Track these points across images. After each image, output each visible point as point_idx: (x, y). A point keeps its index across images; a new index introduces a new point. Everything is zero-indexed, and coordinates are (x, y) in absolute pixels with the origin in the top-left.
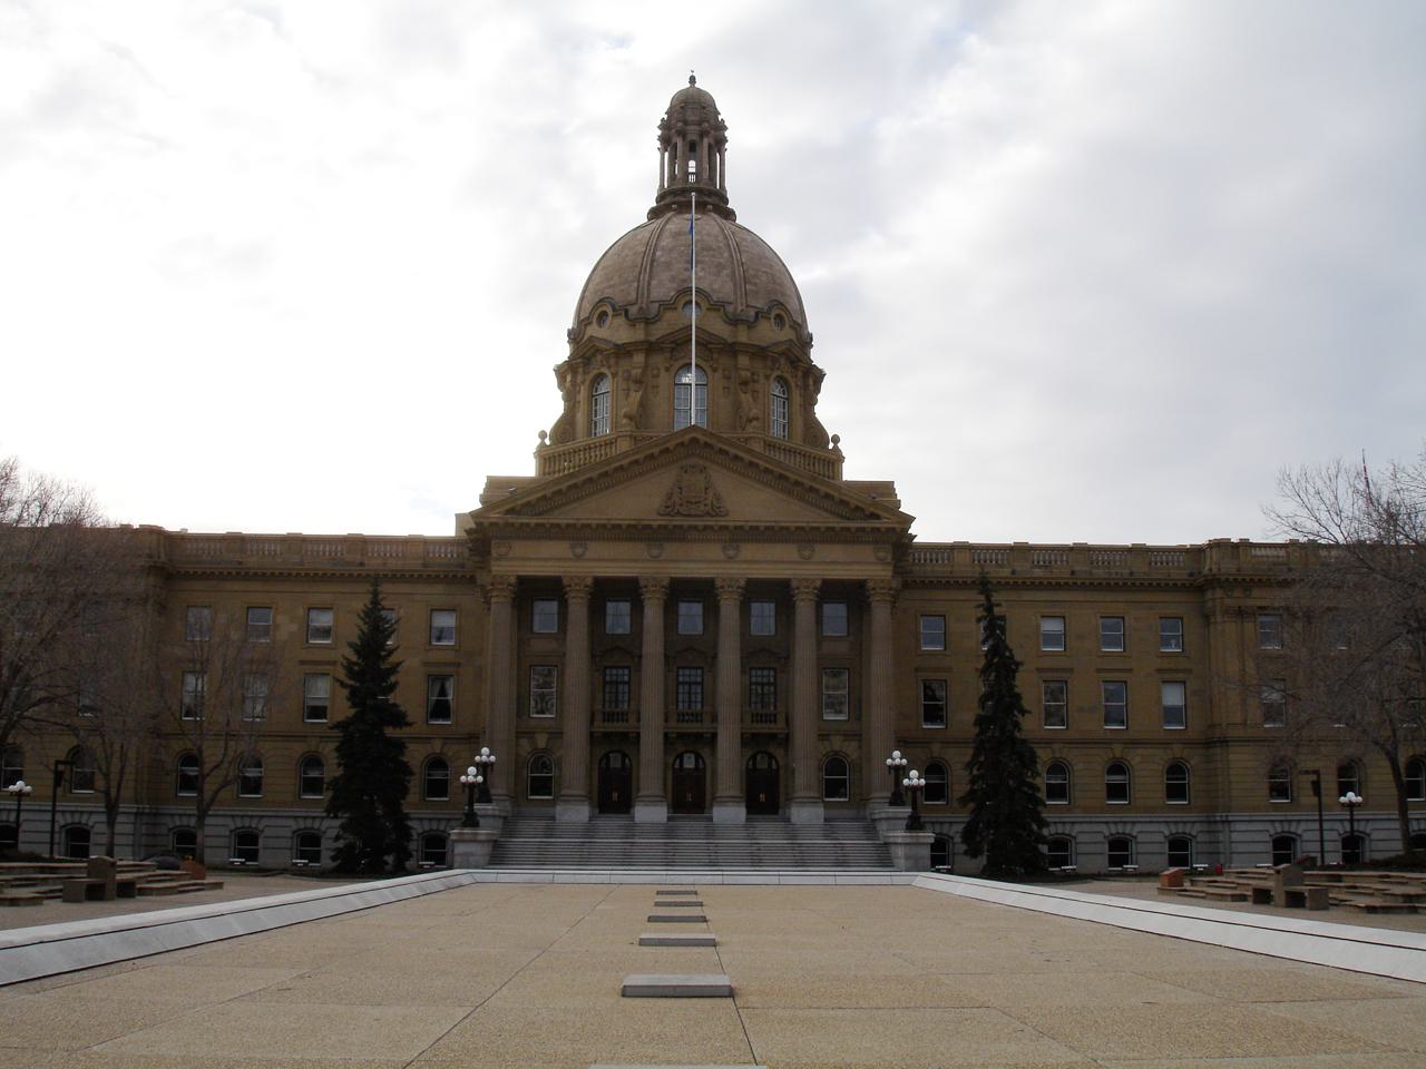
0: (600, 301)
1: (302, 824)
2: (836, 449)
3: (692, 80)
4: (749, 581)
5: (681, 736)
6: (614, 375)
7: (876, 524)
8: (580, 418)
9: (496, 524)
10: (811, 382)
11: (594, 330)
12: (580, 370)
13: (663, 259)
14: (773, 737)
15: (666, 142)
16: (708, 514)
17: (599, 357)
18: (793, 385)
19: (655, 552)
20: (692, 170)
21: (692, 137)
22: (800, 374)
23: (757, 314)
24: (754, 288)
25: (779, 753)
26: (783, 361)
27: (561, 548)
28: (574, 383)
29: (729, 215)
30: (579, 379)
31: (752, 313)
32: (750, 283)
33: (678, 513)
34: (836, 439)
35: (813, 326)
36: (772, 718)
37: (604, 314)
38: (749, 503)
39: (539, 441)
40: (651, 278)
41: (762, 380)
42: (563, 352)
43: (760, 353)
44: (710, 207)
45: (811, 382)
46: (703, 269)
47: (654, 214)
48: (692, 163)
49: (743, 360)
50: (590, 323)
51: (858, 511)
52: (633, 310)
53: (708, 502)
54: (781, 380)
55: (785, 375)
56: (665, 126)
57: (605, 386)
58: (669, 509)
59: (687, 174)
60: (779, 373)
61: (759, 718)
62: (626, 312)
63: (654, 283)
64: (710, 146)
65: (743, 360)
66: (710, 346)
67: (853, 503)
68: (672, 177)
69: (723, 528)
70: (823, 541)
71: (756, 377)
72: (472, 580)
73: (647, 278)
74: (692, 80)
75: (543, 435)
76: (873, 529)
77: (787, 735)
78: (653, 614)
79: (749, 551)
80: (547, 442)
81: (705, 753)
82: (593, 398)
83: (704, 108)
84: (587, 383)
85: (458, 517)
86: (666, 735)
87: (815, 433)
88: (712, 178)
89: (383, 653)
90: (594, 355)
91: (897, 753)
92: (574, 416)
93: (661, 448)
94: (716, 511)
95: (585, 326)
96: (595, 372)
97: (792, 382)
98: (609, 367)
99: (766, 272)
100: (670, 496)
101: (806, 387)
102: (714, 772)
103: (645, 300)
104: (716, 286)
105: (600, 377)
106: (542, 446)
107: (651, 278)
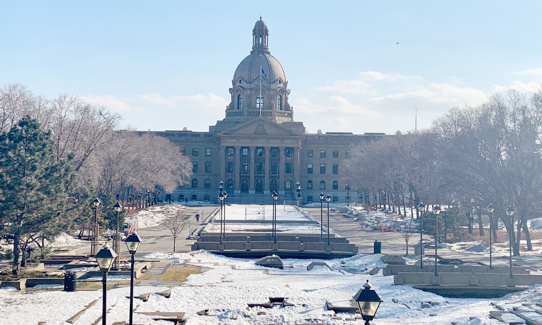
1: (180, 193)
2: (292, 110)
3: (261, 18)
4: (271, 147)
5: (258, 176)
14: (276, 177)
15: (253, 35)
19: (253, 141)
20: (260, 42)
21: (261, 34)
25: (277, 180)
28: (234, 94)
29: (269, 53)
34: (292, 108)
36: (276, 173)
39: (226, 108)
47: (251, 52)
49: (272, 92)
55: (281, 94)
56: (254, 31)
58: (256, 134)
59: (259, 43)
61: (272, 173)
72: (215, 142)
74: (261, 18)
75: (227, 107)
77: (279, 177)
78: (252, 153)
81: (262, 179)
85: (210, 126)
86: (255, 176)
91: (298, 182)
92: (234, 103)
102: (264, 183)
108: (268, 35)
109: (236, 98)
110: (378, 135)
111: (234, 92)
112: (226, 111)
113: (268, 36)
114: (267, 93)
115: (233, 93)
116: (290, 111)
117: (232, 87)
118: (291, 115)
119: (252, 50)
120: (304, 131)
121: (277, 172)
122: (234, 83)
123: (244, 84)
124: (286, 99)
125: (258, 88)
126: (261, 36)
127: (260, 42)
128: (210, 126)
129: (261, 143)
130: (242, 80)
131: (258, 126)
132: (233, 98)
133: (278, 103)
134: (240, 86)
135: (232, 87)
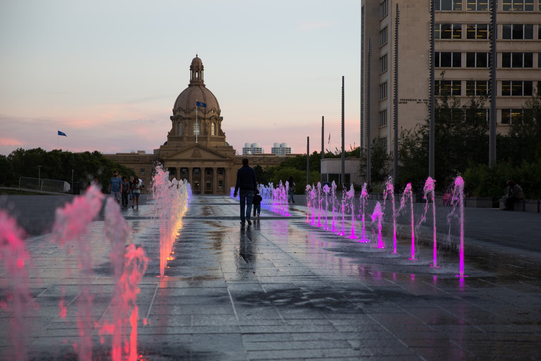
2: (225, 136)
3: (197, 55)
8: (176, 129)
11: (178, 113)
12: (176, 121)
15: (191, 70)
17: (179, 119)
20: (197, 76)
27: (175, 163)
28: (174, 122)
30: (176, 122)
34: (224, 133)
35: (221, 108)
37: (180, 110)
38: (206, 155)
43: (210, 119)
47: (189, 85)
49: (207, 121)
54: (214, 123)
57: (181, 124)
58: (193, 156)
59: (196, 77)
61: (207, 189)
65: (207, 121)
69: (202, 160)
70: (218, 161)
74: (197, 55)
75: (169, 133)
79: (206, 163)
82: (178, 126)
85: (154, 150)
87: (221, 134)
94: (200, 157)
100: (193, 154)
101: (219, 123)
105: (179, 122)
108: (203, 70)
109: (176, 125)
110: (268, 156)
111: (174, 120)
112: (168, 137)
113: (204, 71)
114: (203, 121)
116: (223, 136)
117: (172, 115)
118: (223, 139)
119: (190, 83)
120: (234, 153)
121: (211, 188)
122: (174, 111)
123: (183, 114)
124: (220, 125)
125: (195, 117)
126: (197, 71)
127: (197, 76)
128: (154, 150)
129: (197, 165)
131: (194, 152)
132: (173, 125)
134: (180, 116)
135: (172, 115)
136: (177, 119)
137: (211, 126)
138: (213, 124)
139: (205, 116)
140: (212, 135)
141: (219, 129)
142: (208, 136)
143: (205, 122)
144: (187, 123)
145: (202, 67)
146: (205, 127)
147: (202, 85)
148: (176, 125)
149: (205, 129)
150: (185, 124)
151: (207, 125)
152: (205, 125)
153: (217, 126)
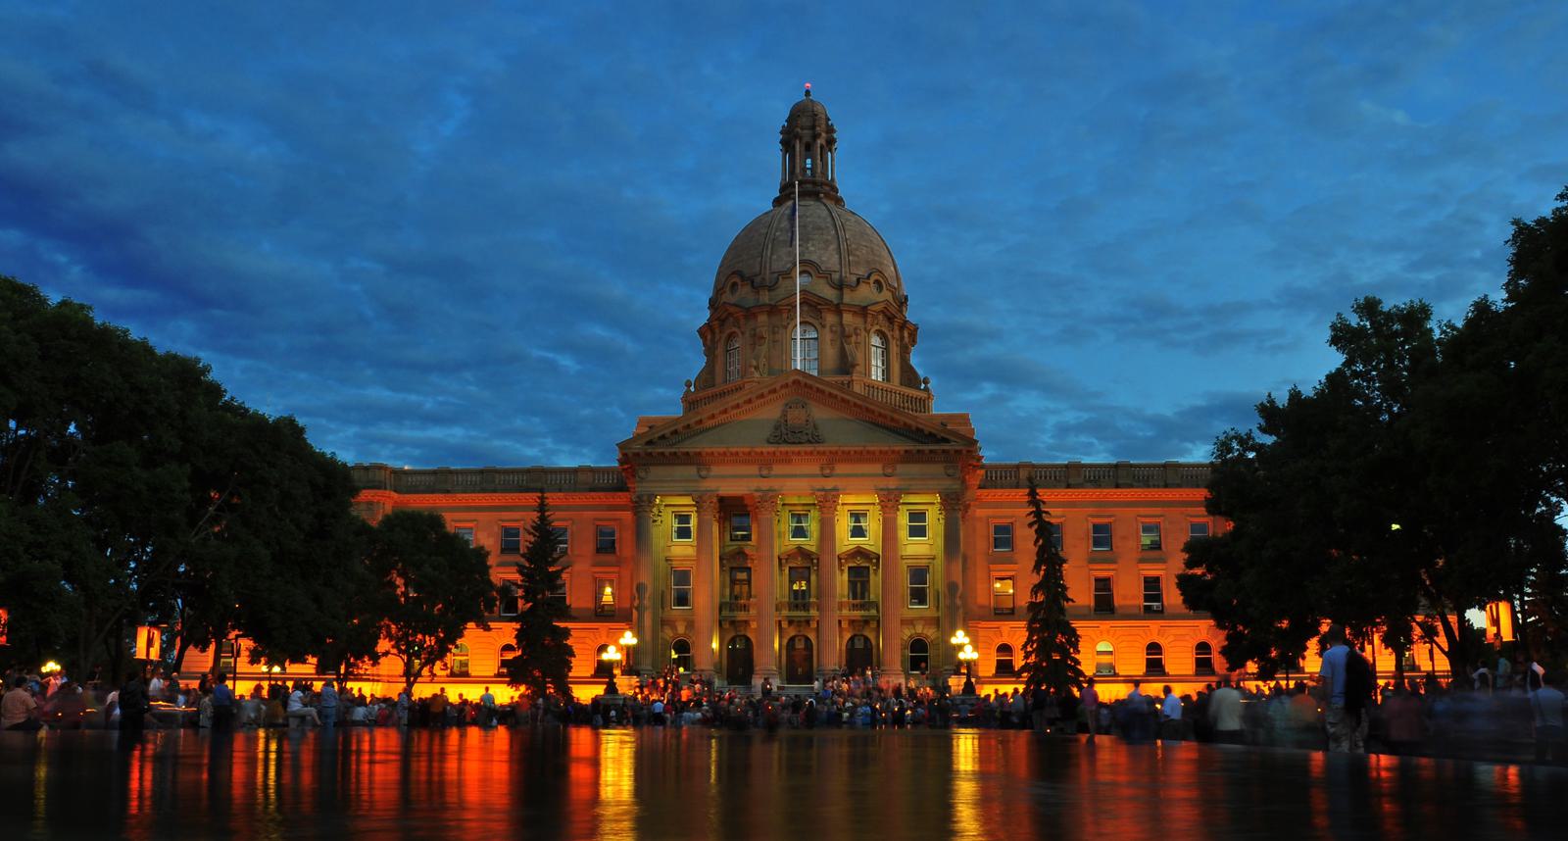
0: (733, 273)
2: (926, 389)
3: (808, 93)
6: (743, 333)
7: (946, 447)
8: (719, 369)
9: (638, 454)
10: (906, 334)
11: (728, 297)
13: (781, 238)
16: (809, 442)
18: (889, 337)
19: (765, 472)
22: (896, 327)
23: (858, 280)
24: (856, 259)
26: (881, 317)
29: (839, 201)
30: (717, 337)
31: (854, 279)
32: (854, 255)
33: (785, 442)
37: (734, 285)
40: (772, 254)
41: (863, 333)
42: (704, 316)
44: (822, 195)
45: (906, 334)
46: (813, 245)
48: (809, 161)
49: (848, 318)
50: (725, 292)
51: (932, 438)
52: (758, 280)
53: (809, 432)
54: (881, 334)
60: (877, 327)
62: (753, 282)
63: (774, 257)
64: (822, 147)
65: (848, 318)
66: (819, 307)
67: (927, 430)
68: (792, 172)
71: (858, 331)
73: (769, 254)
74: (808, 93)
75: (688, 384)
76: (944, 451)
80: (692, 389)
83: (816, 115)
84: (722, 341)
88: (824, 173)
89: (550, 559)
90: (727, 318)
93: (770, 388)
95: (721, 294)
96: (728, 331)
97: (889, 334)
98: (739, 328)
99: (866, 246)
100: (777, 428)
103: (768, 272)
104: (824, 259)
106: (688, 393)
107: (772, 254)
108: (831, 142)
111: (713, 333)
114: (830, 319)
115: (709, 337)
116: (919, 389)
130: (737, 279)
132: (710, 352)
133: (873, 362)
136: (723, 322)
137: (867, 346)
138: (876, 340)
139: (841, 296)
140: (873, 378)
141: (902, 368)
142: (855, 377)
143: (841, 324)
144: (764, 331)
145: (830, 130)
146: (842, 343)
147: (827, 195)
148: (719, 351)
149: (843, 354)
150: (755, 335)
151: (849, 336)
152: (843, 336)
153: (895, 349)
